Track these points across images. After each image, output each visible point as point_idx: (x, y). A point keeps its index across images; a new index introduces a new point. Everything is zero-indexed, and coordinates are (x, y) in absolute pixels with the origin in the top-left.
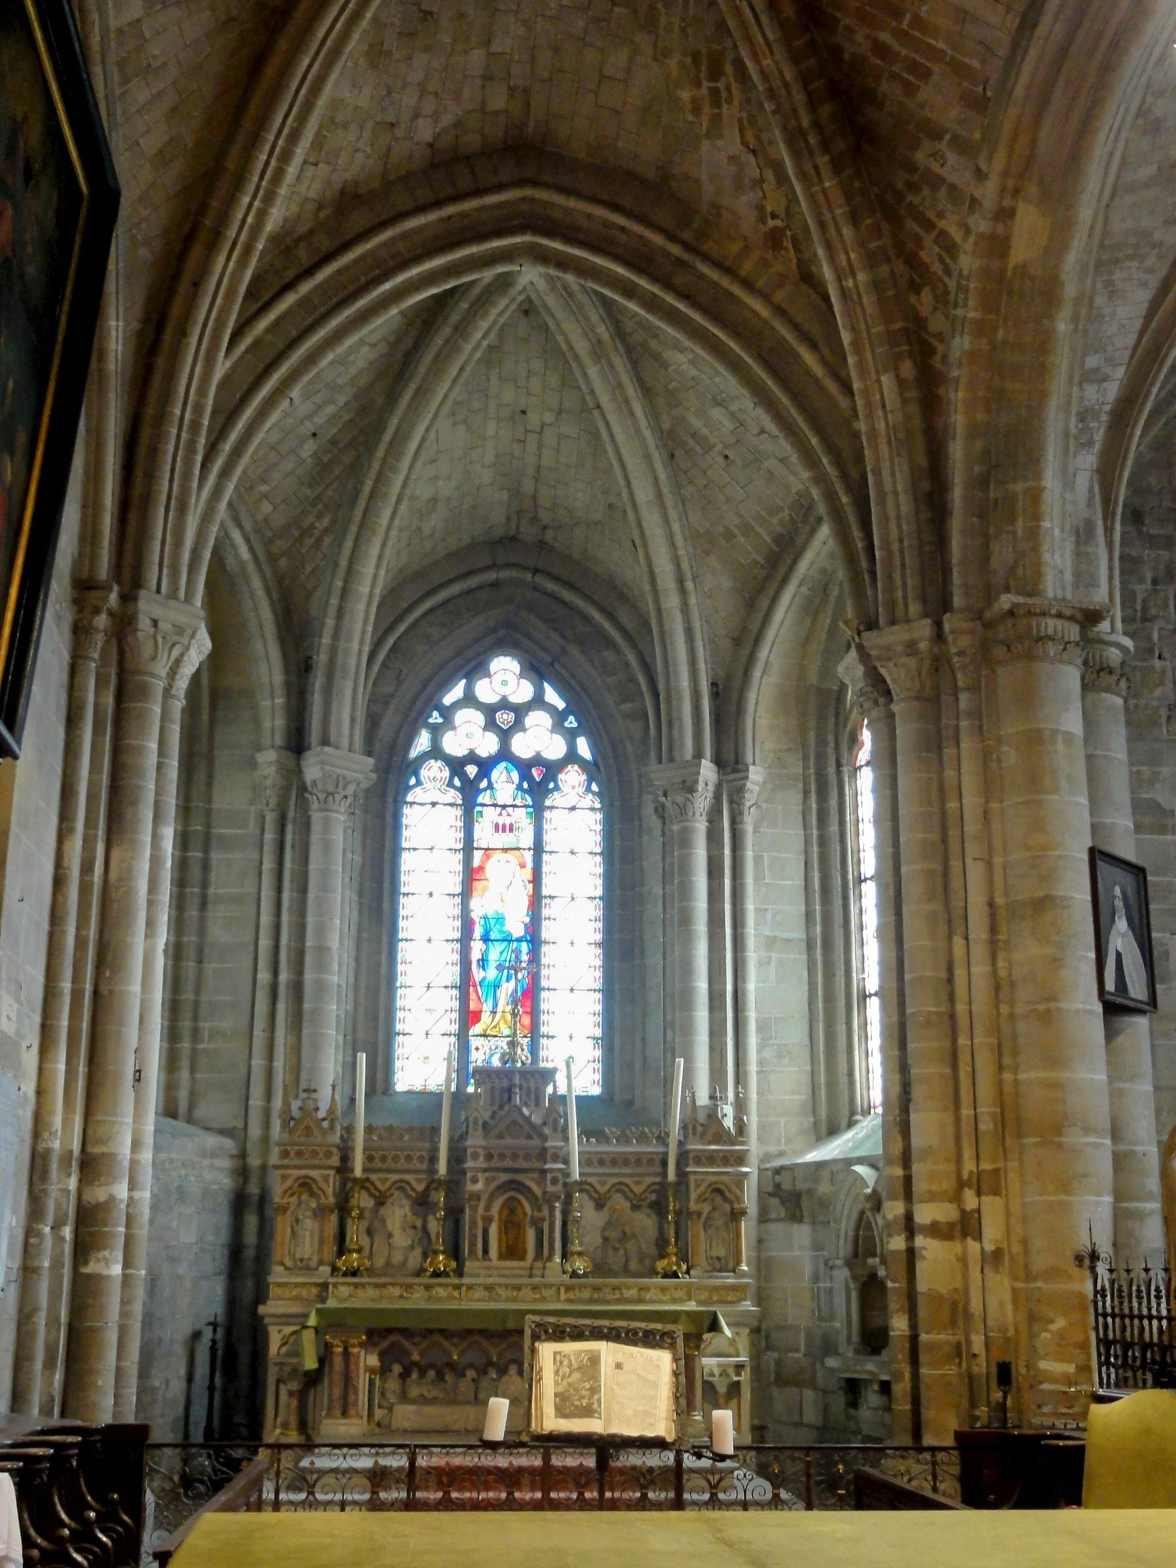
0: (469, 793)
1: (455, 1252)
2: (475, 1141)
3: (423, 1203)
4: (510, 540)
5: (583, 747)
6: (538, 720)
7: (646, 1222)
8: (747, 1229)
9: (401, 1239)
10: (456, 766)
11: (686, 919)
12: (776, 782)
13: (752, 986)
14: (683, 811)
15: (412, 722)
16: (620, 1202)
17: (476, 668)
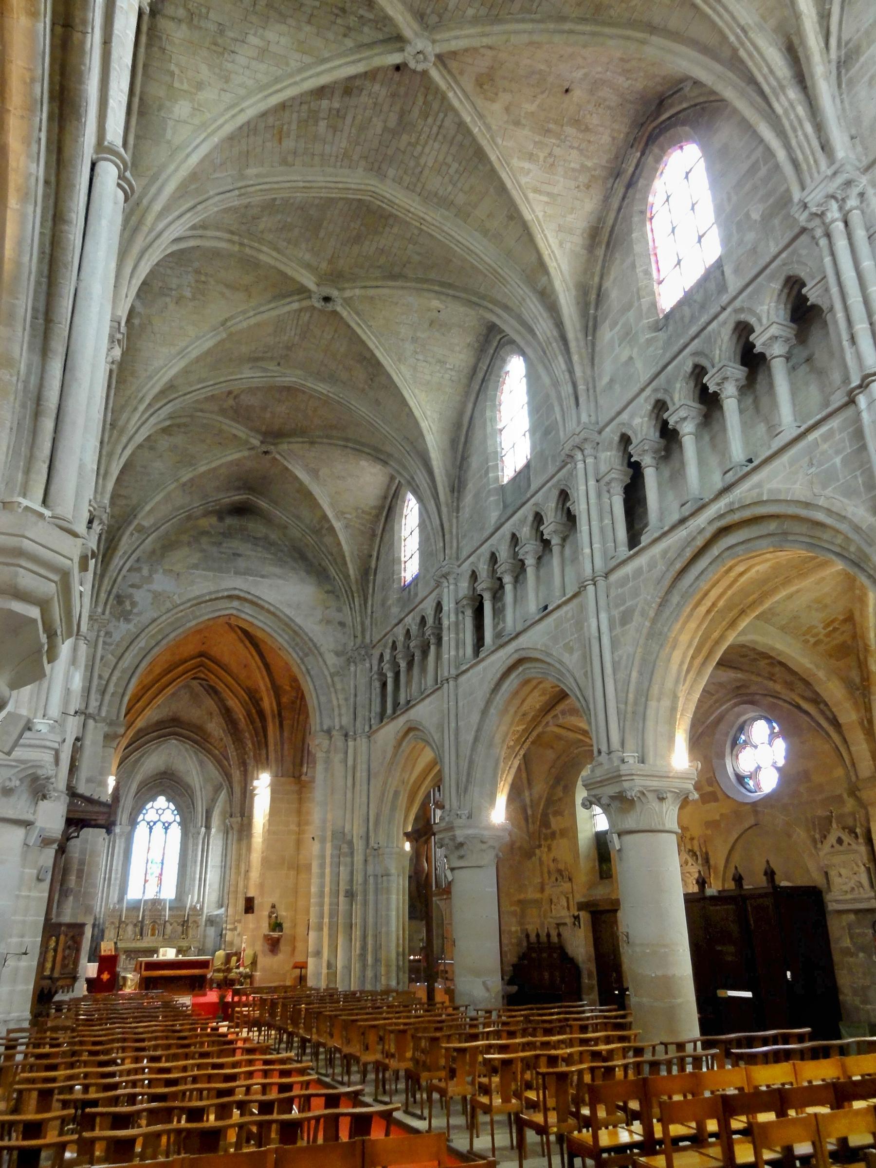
0: (151, 828)
1: (141, 935)
2: (147, 913)
3: (135, 925)
4: (165, 773)
5: (178, 818)
6: (168, 812)
7: (180, 929)
8: (201, 929)
9: (130, 933)
10: (148, 823)
11: (196, 862)
12: (218, 831)
13: (208, 876)
14: (197, 838)
15: (139, 812)
16: (175, 924)
17: (154, 799)
